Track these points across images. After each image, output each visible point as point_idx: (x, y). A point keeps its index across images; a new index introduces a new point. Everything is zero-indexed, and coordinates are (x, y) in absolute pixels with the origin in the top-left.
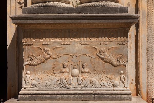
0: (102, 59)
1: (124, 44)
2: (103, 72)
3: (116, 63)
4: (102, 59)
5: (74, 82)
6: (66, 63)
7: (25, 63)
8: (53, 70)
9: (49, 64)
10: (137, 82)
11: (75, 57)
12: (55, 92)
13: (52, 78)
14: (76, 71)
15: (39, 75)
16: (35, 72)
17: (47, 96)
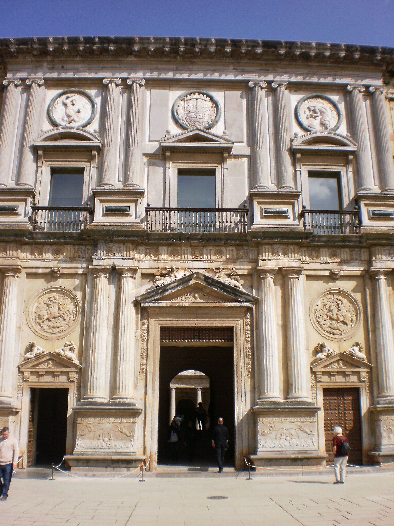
0: (121, 432)
1: (134, 423)
2: (121, 440)
3: (128, 434)
4: (121, 432)
5: (105, 444)
6: (101, 435)
7: (78, 434)
8: (93, 438)
9: (91, 435)
10: (145, 448)
11: (106, 431)
12: (94, 451)
13: (92, 442)
14: (106, 439)
15: (85, 441)
16: (83, 439)
17: (90, 453)
